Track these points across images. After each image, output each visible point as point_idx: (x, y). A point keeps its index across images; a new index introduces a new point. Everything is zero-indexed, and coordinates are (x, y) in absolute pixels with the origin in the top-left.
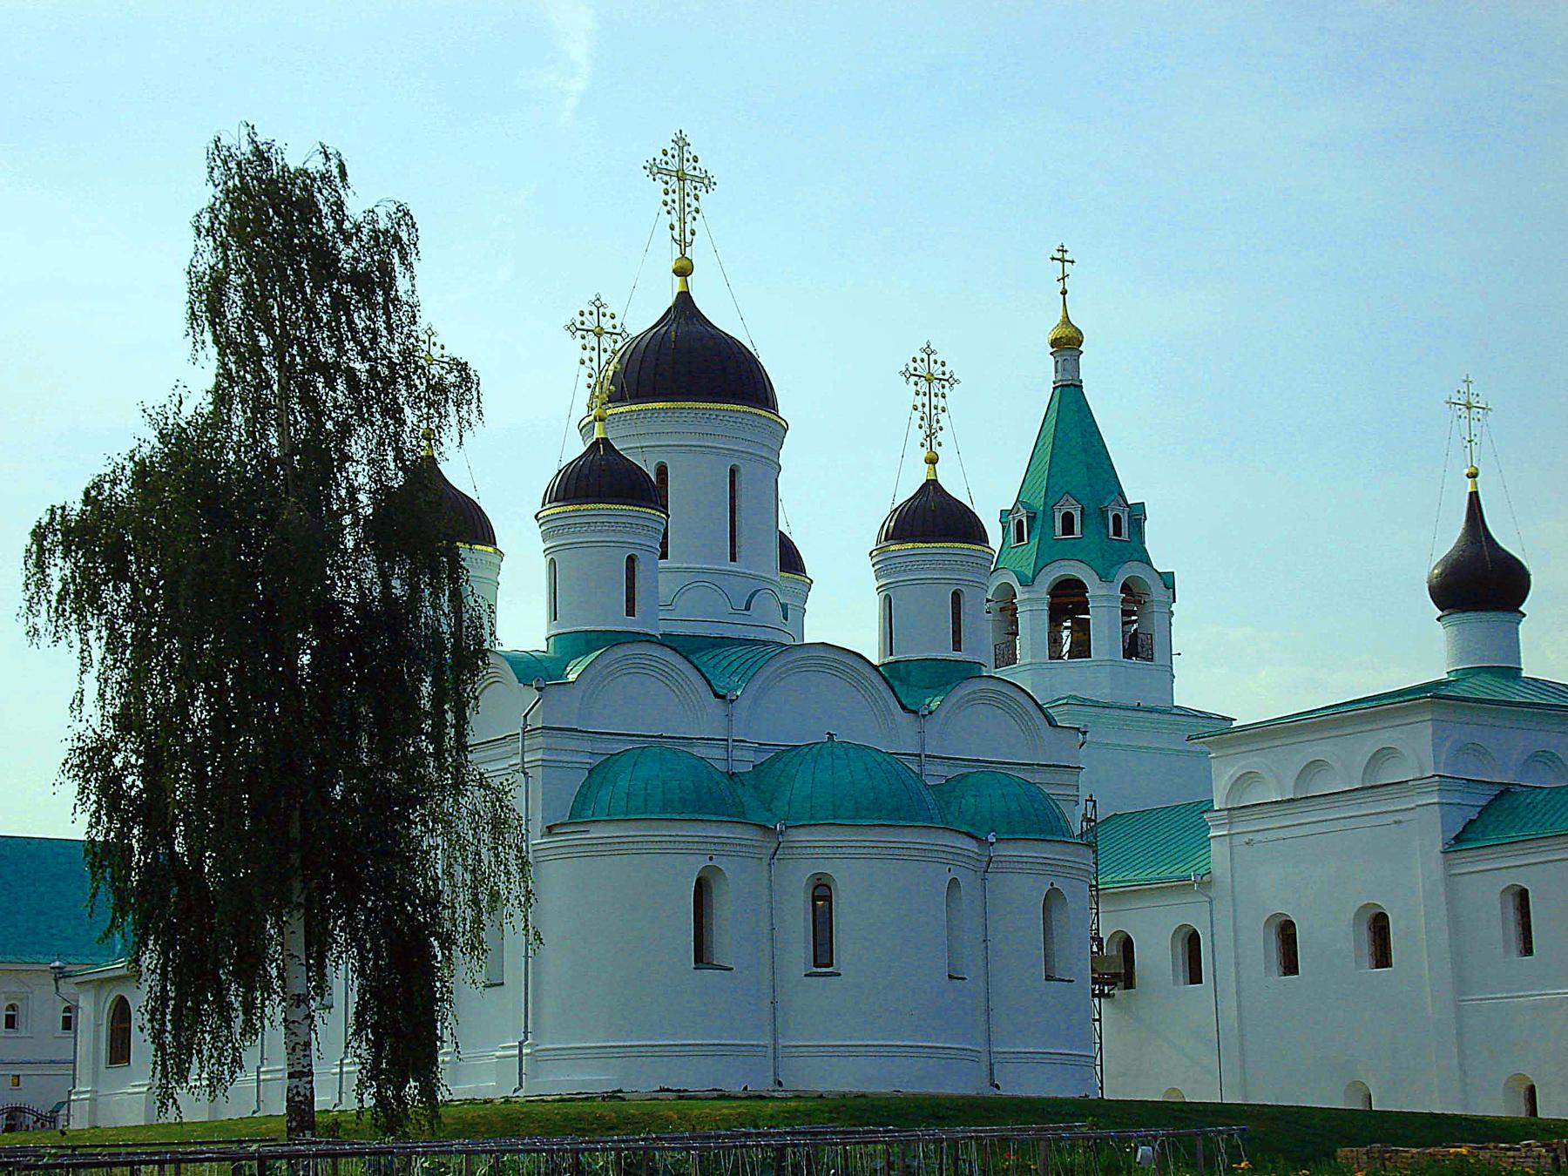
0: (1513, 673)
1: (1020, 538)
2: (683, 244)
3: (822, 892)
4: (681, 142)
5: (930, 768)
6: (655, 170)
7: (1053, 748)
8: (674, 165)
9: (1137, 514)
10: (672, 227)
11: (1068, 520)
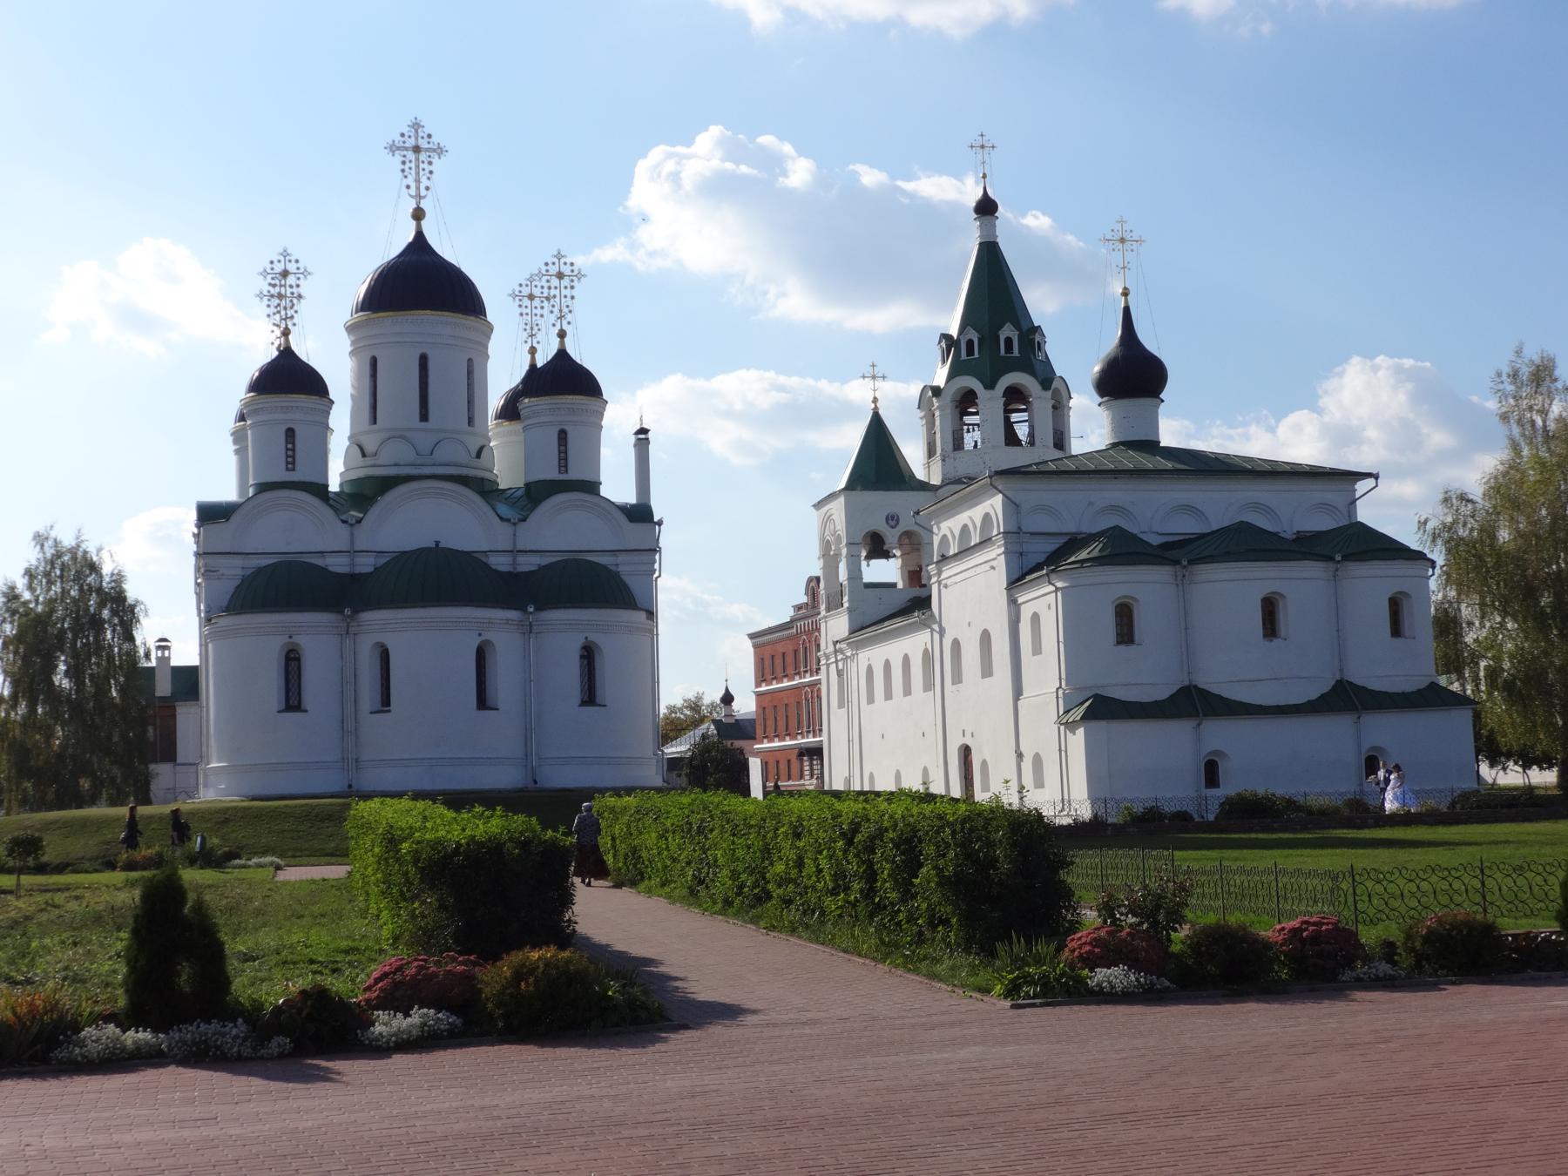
0: (1150, 446)
1: (944, 362)
2: (419, 197)
3: (385, 656)
5: (521, 559)
6: (393, 148)
8: (411, 143)
9: (1031, 336)
11: (970, 343)
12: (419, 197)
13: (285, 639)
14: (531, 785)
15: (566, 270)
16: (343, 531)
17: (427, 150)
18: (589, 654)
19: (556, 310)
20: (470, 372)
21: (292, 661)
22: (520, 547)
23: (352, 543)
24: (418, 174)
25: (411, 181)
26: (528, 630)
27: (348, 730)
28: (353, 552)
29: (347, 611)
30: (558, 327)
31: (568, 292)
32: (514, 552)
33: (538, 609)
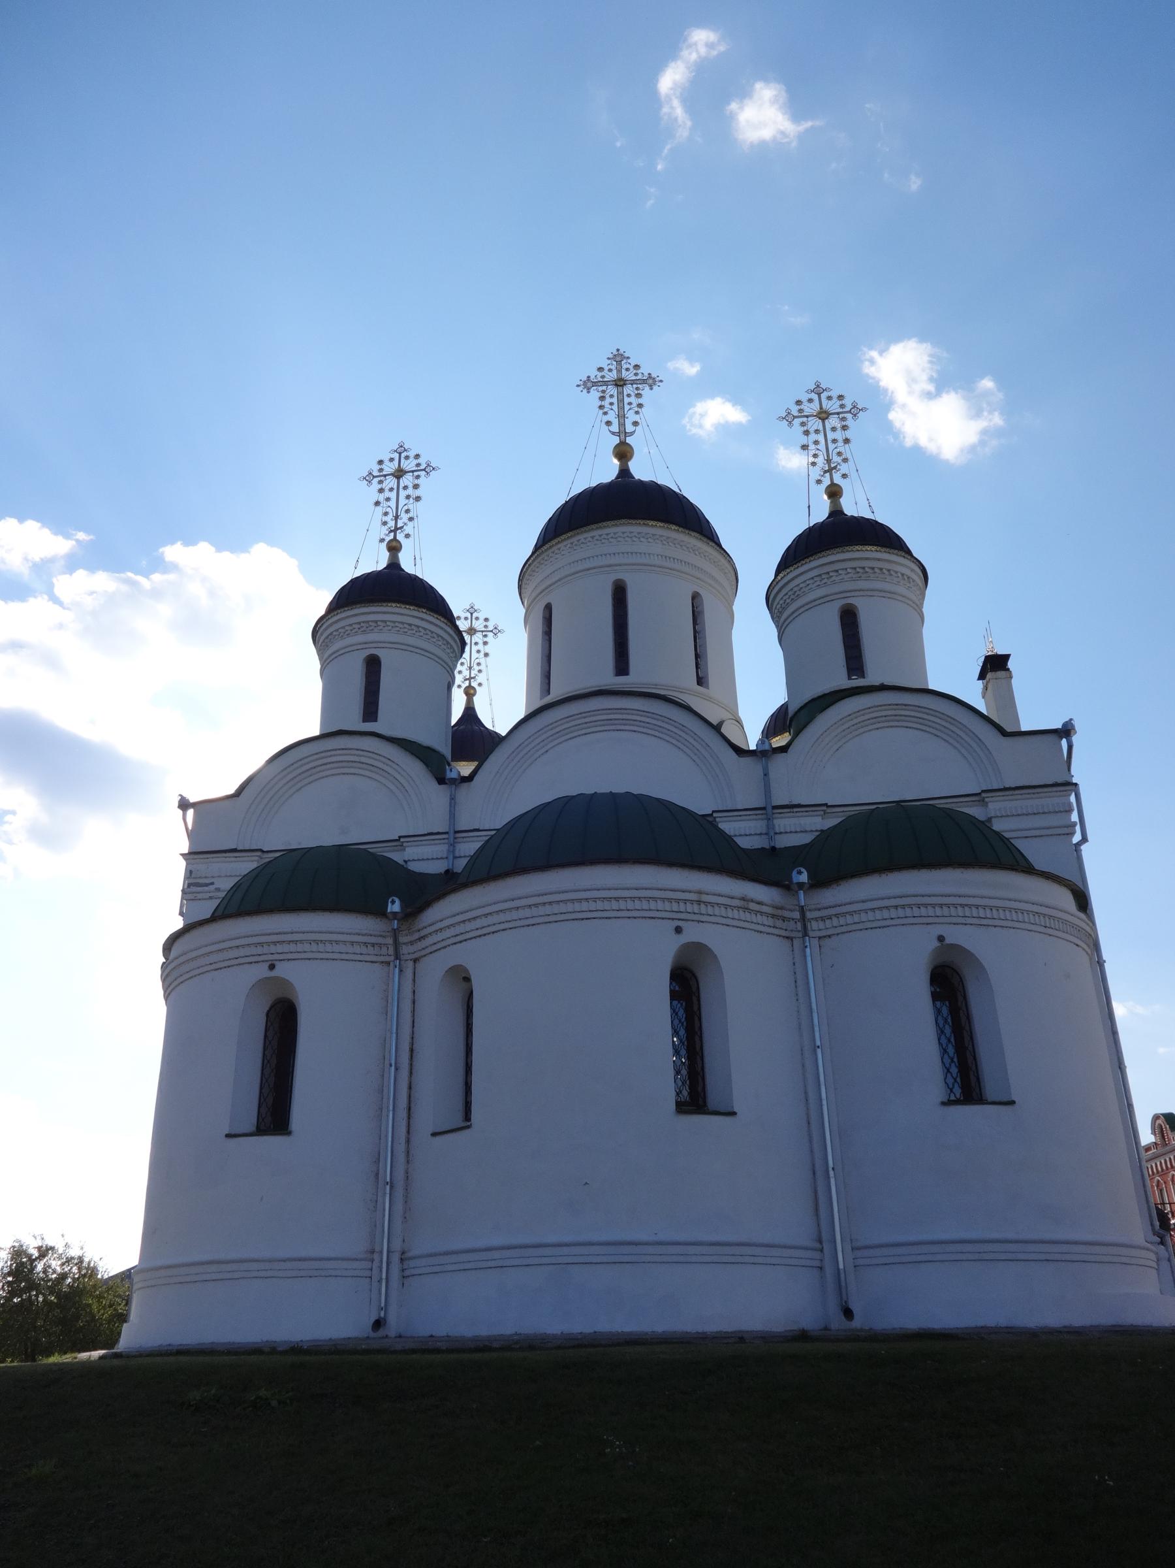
2: (623, 433)
4: (619, 358)
5: (783, 822)
6: (588, 384)
7: (1014, 765)
10: (608, 423)
12: (623, 433)
13: (262, 971)
14: (838, 1323)
15: (832, 406)
16: (437, 796)
17: (633, 382)
18: (949, 983)
19: (821, 460)
20: (697, 616)
21: (282, 1023)
22: (780, 799)
23: (452, 815)
24: (621, 408)
25: (612, 416)
26: (799, 930)
27: (392, 1180)
28: (454, 835)
29: (395, 907)
30: (827, 481)
31: (839, 435)
32: (768, 811)
33: (820, 882)
